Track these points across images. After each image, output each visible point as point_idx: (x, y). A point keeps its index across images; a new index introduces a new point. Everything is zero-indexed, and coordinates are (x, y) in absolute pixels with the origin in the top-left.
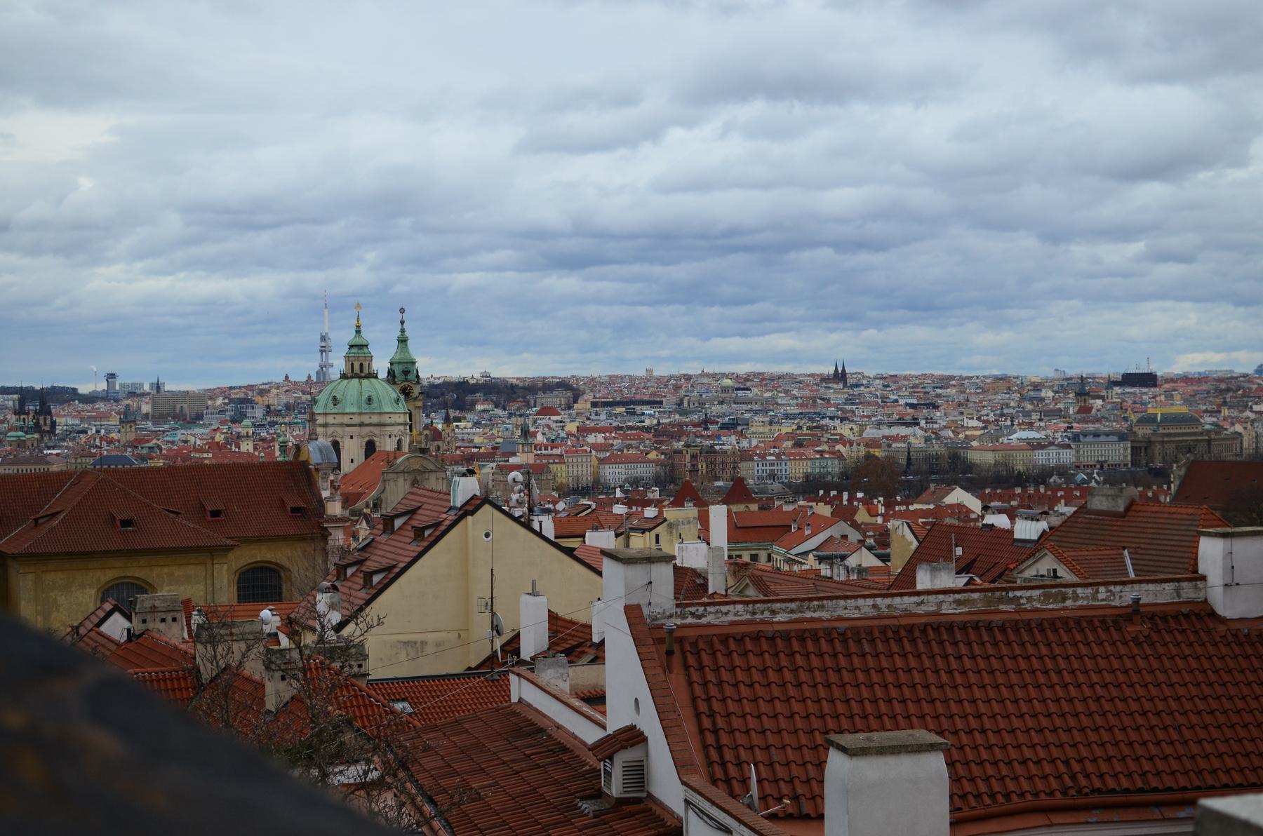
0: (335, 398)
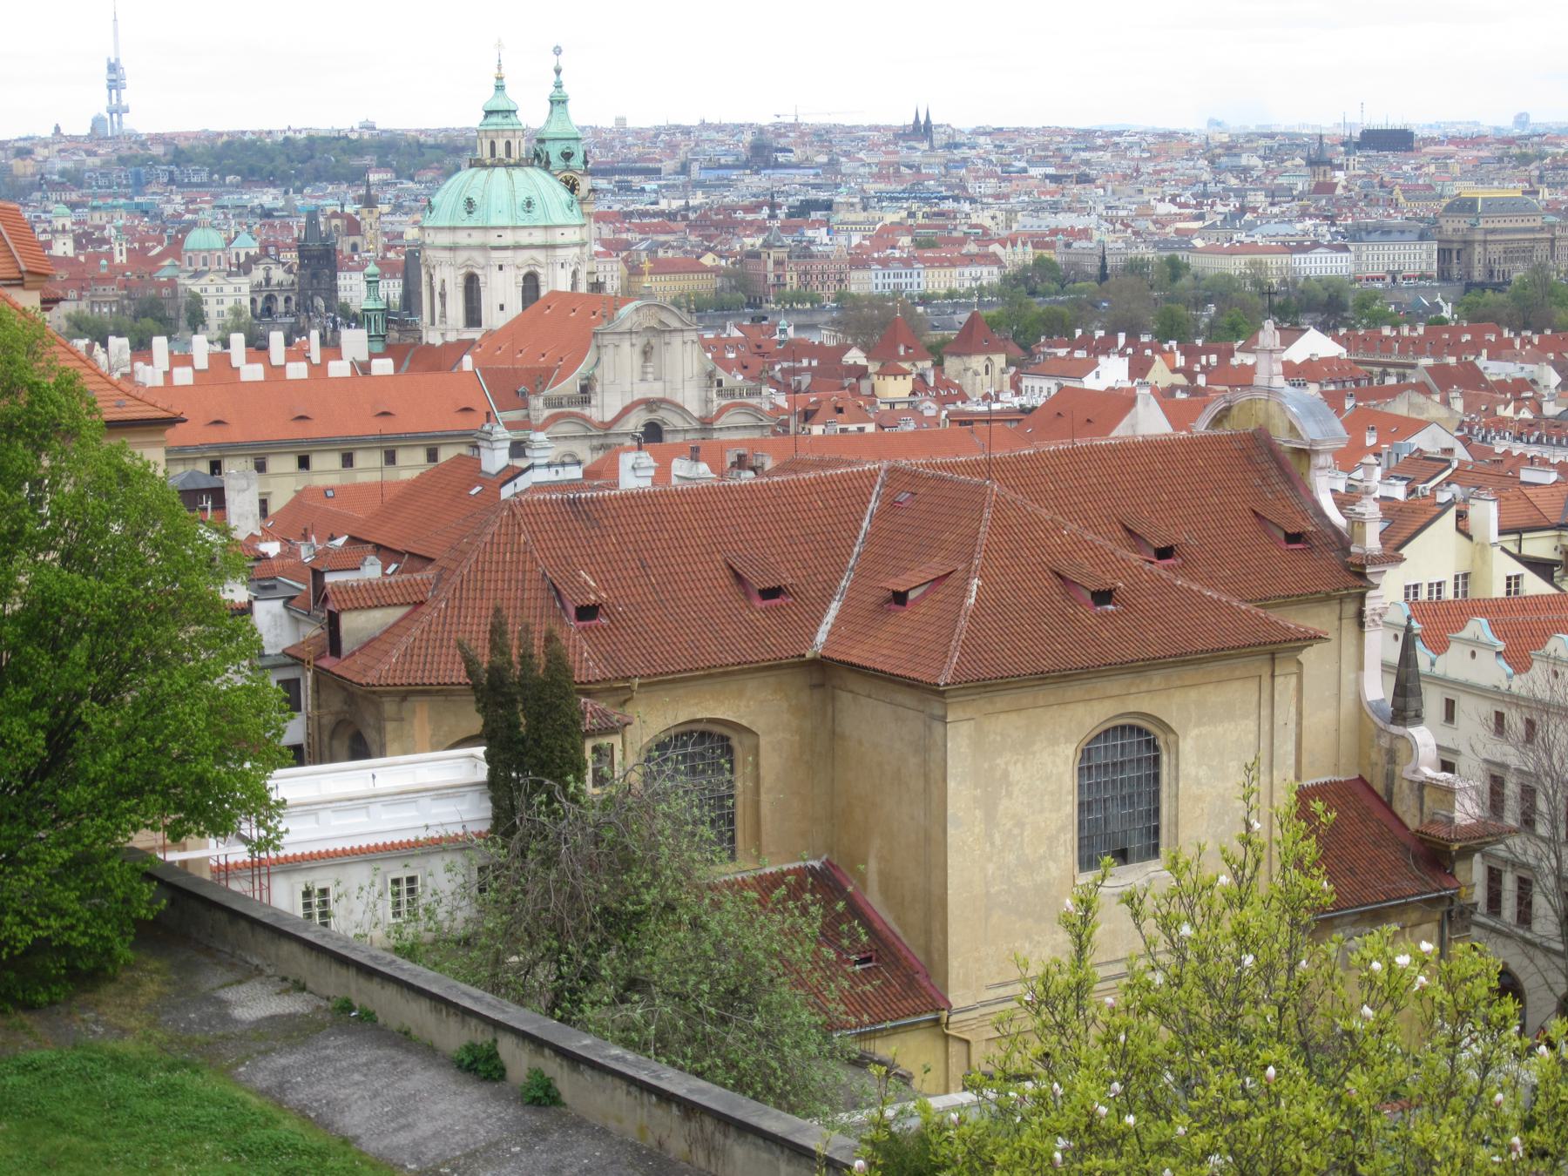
0: (470, 203)
